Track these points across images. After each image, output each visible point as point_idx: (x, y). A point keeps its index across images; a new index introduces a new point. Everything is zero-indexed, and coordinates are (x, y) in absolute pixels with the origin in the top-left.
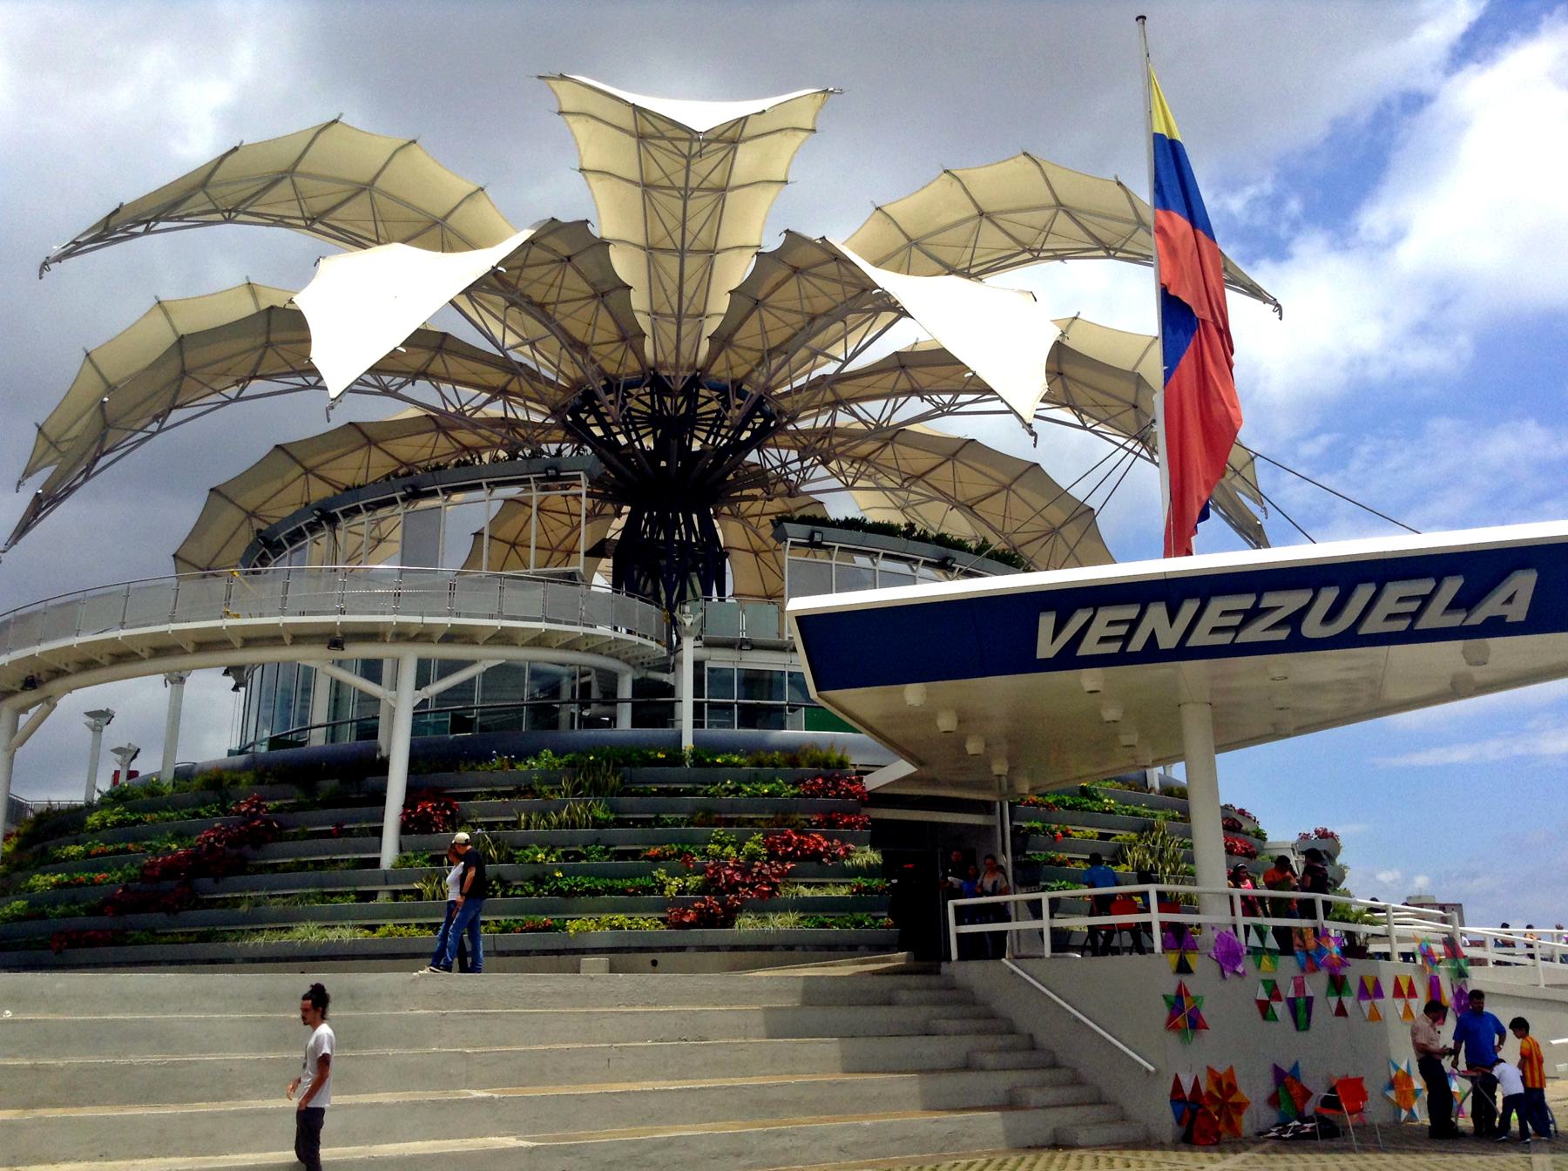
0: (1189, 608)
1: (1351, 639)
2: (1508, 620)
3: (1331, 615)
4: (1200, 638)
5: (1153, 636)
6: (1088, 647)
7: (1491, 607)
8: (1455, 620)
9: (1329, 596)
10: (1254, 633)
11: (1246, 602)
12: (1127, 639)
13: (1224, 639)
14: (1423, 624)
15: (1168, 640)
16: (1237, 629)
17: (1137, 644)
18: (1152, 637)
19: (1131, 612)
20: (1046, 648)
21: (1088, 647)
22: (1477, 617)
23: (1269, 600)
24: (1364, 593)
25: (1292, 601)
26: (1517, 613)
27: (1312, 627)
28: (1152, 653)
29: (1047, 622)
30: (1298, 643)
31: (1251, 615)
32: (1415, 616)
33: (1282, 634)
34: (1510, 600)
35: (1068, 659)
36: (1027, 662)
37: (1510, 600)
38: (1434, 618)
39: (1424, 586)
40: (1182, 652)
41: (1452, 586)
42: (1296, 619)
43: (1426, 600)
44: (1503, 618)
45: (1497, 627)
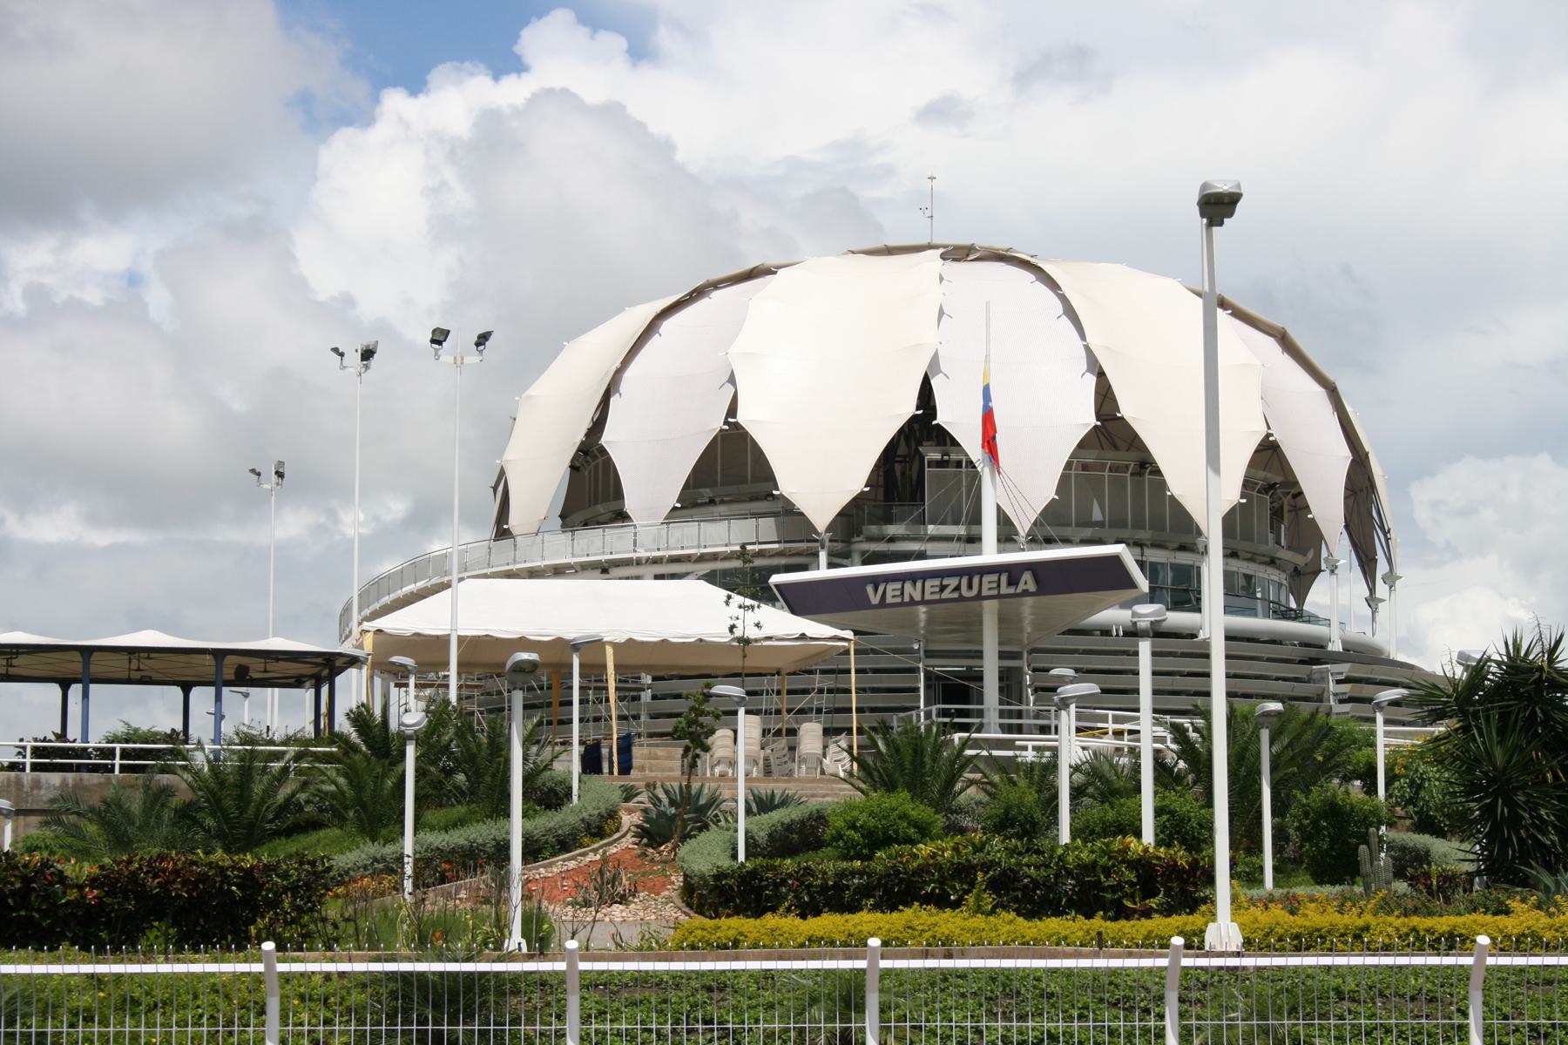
0: (919, 584)
3: (970, 587)
4: (928, 597)
8: (1011, 590)
9: (965, 581)
10: (946, 595)
11: (937, 582)
12: (902, 593)
13: (937, 597)
15: (917, 597)
17: (907, 599)
18: (911, 597)
19: (898, 585)
20: (875, 600)
21: (889, 600)
22: (1019, 590)
23: (945, 582)
24: (976, 580)
25: (953, 582)
26: (1032, 587)
27: (965, 592)
29: (870, 589)
31: (943, 588)
32: (999, 586)
33: (956, 595)
34: (1026, 583)
36: (864, 604)
37: (1026, 583)
38: (1005, 590)
41: (1004, 578)
42: (958, 588)
45: (1026, 593)
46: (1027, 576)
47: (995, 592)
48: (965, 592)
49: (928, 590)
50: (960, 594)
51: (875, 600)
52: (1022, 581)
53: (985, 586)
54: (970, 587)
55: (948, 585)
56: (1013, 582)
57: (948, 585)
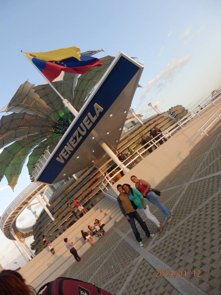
1: (89, 131)
2: (102, 111)
3: (83, 131)
4: (75, 146)
5: (70, 151)
6: (66, 157)
7: (97, 113)
10: (79, 140)
11: (72, 138)
12: (67, 153)
13: (76, 144)
14: (93, 122)
15: (72, 150)
16: (76, 141)
19: (63, 150)
20: (63, 161)
21: (66, 157)
22: (98, 115)
23: (74, 135)
25: (76, 134)
28: (73, 153)
30: (84, 137)
31: (75, 138)
32: (91, 121)
33: (81, 137)
34: (98, 109)
35: (66, 161)
36: (61, 166)
37: (98, 109)
38: (94, 119)
39: (86, 118)
40: (76, 149)
41: (89, 114)
42: (80, 135)
43: (89, 118)
44: (100, 112)
45: (102, 114)
46: (96, 105)
47: (91, 124)
48: (83, 133)
49: (72, 143)
50: (82, 136)
51: (63, 161)
52: (96, 110)
53: (86, 124)
54: (83, 131)
55: (76, 136)
56: (93, 114)
57: (76, 136)
